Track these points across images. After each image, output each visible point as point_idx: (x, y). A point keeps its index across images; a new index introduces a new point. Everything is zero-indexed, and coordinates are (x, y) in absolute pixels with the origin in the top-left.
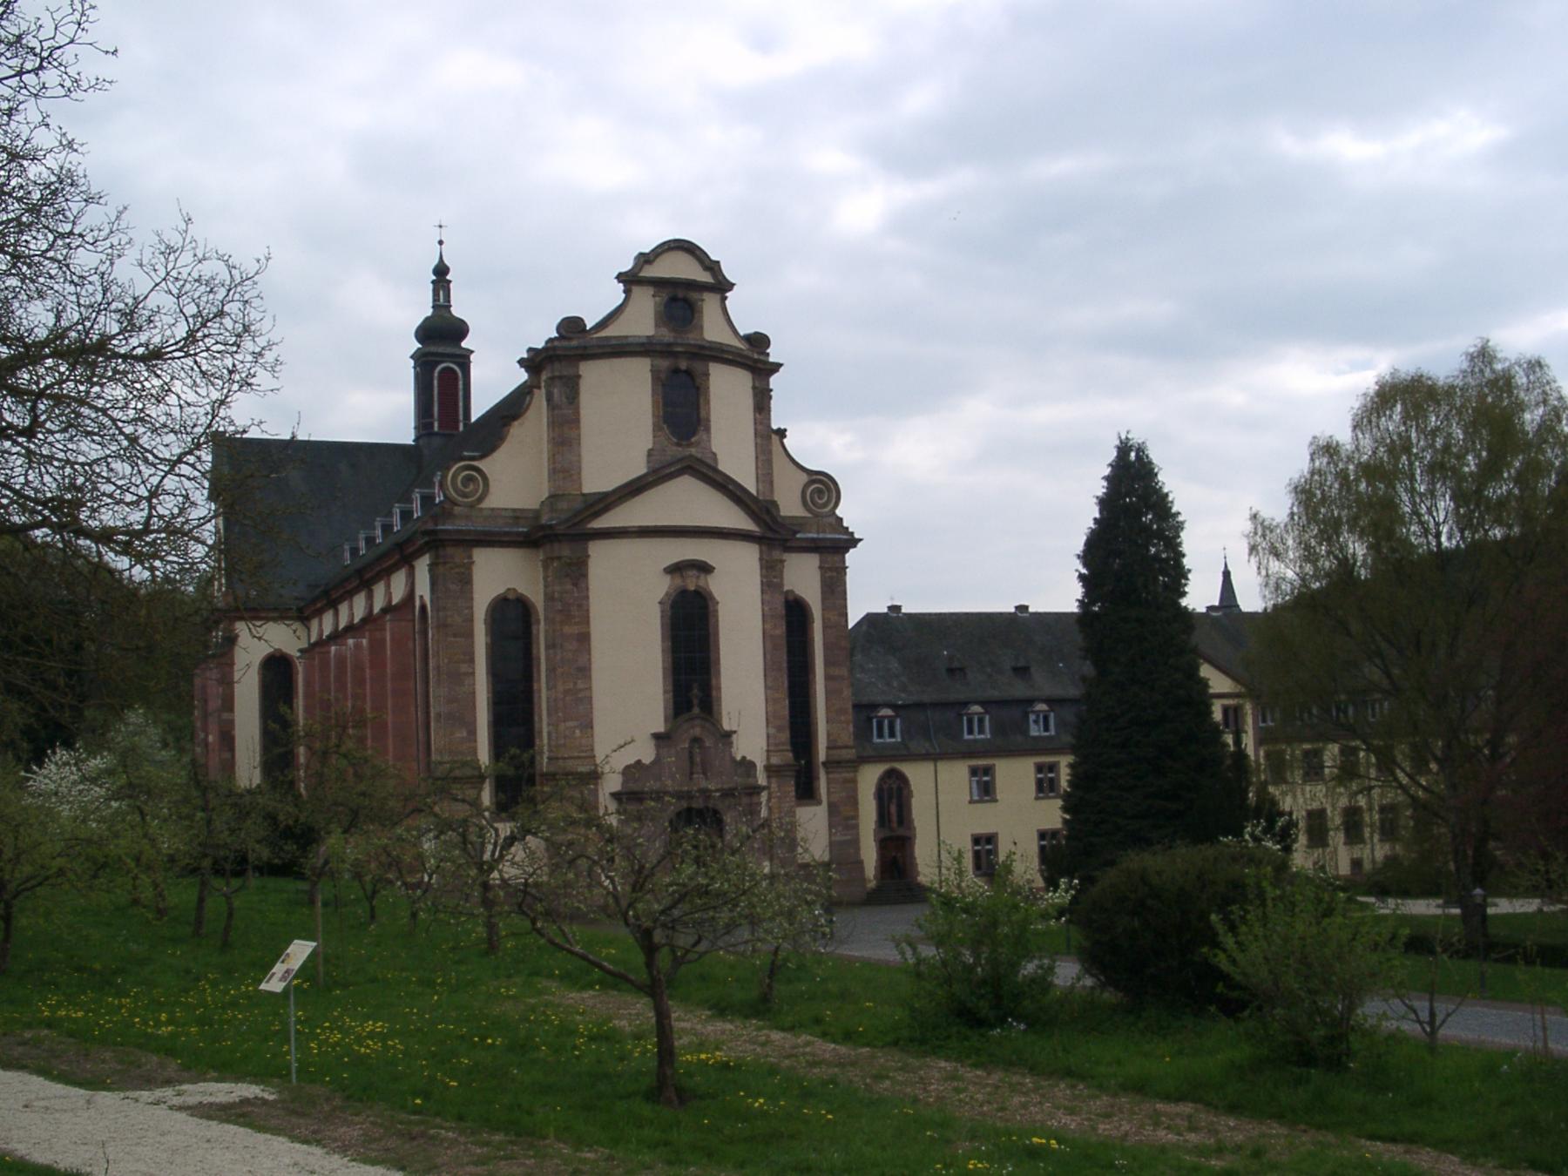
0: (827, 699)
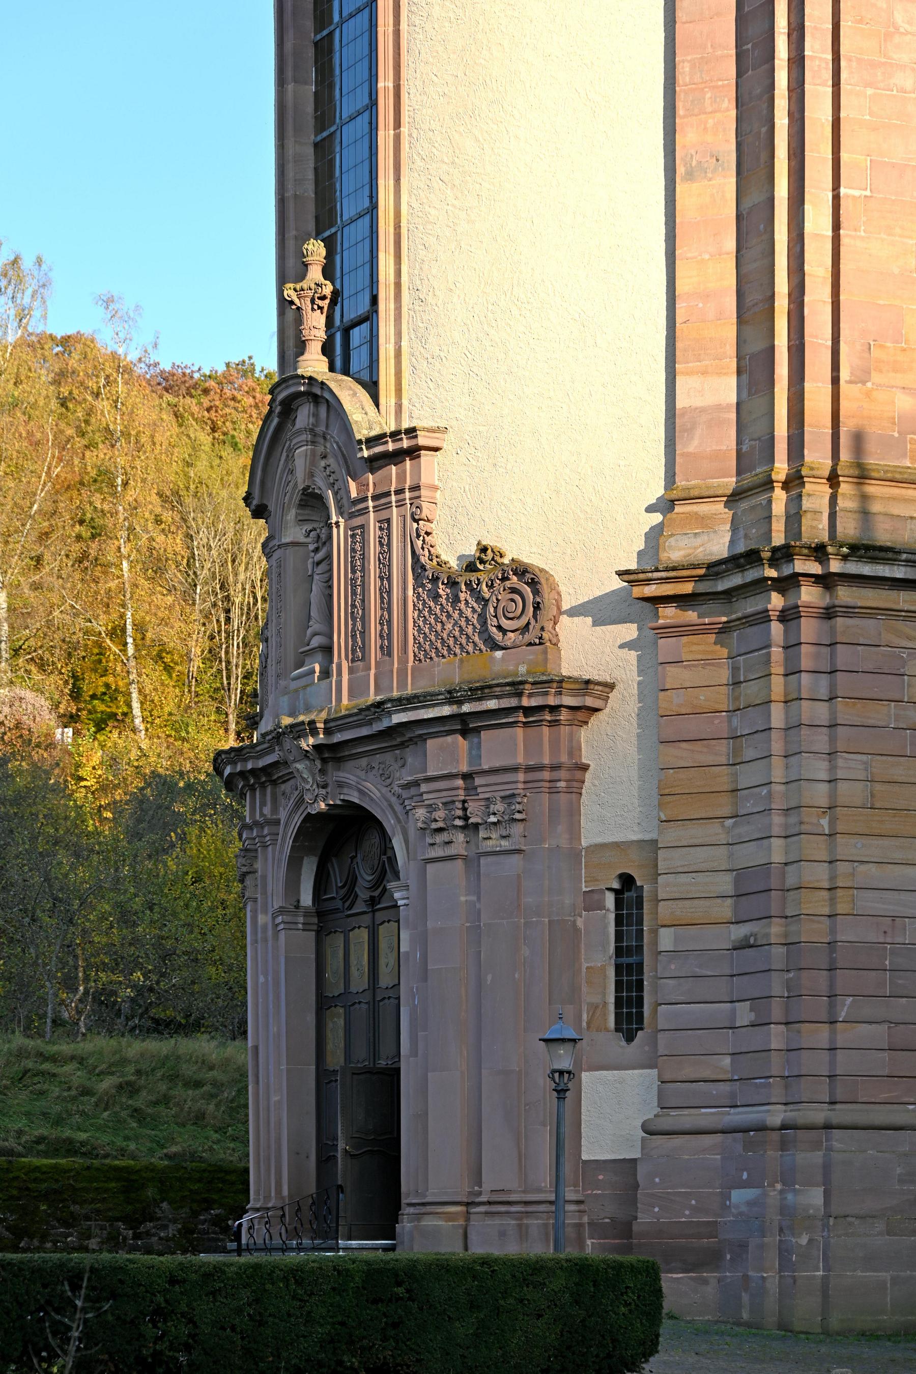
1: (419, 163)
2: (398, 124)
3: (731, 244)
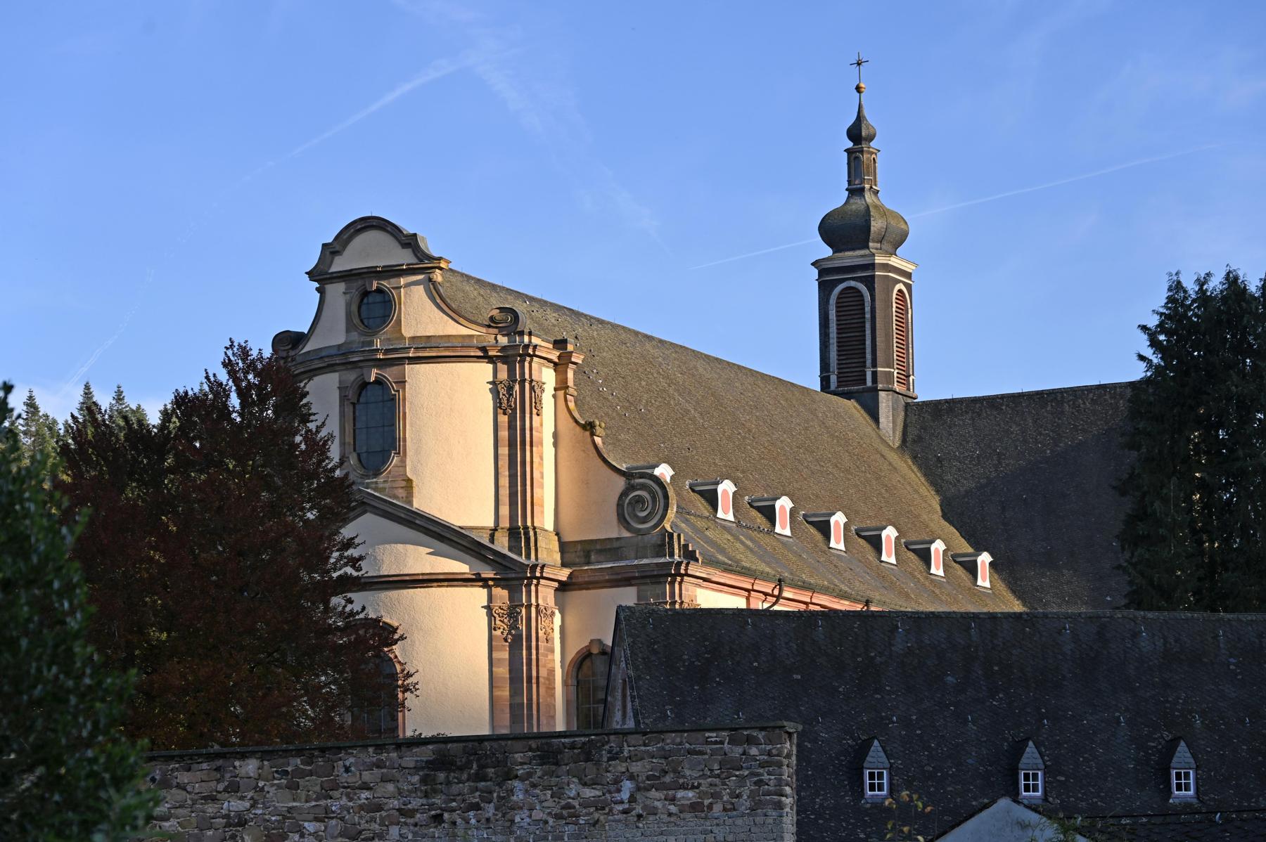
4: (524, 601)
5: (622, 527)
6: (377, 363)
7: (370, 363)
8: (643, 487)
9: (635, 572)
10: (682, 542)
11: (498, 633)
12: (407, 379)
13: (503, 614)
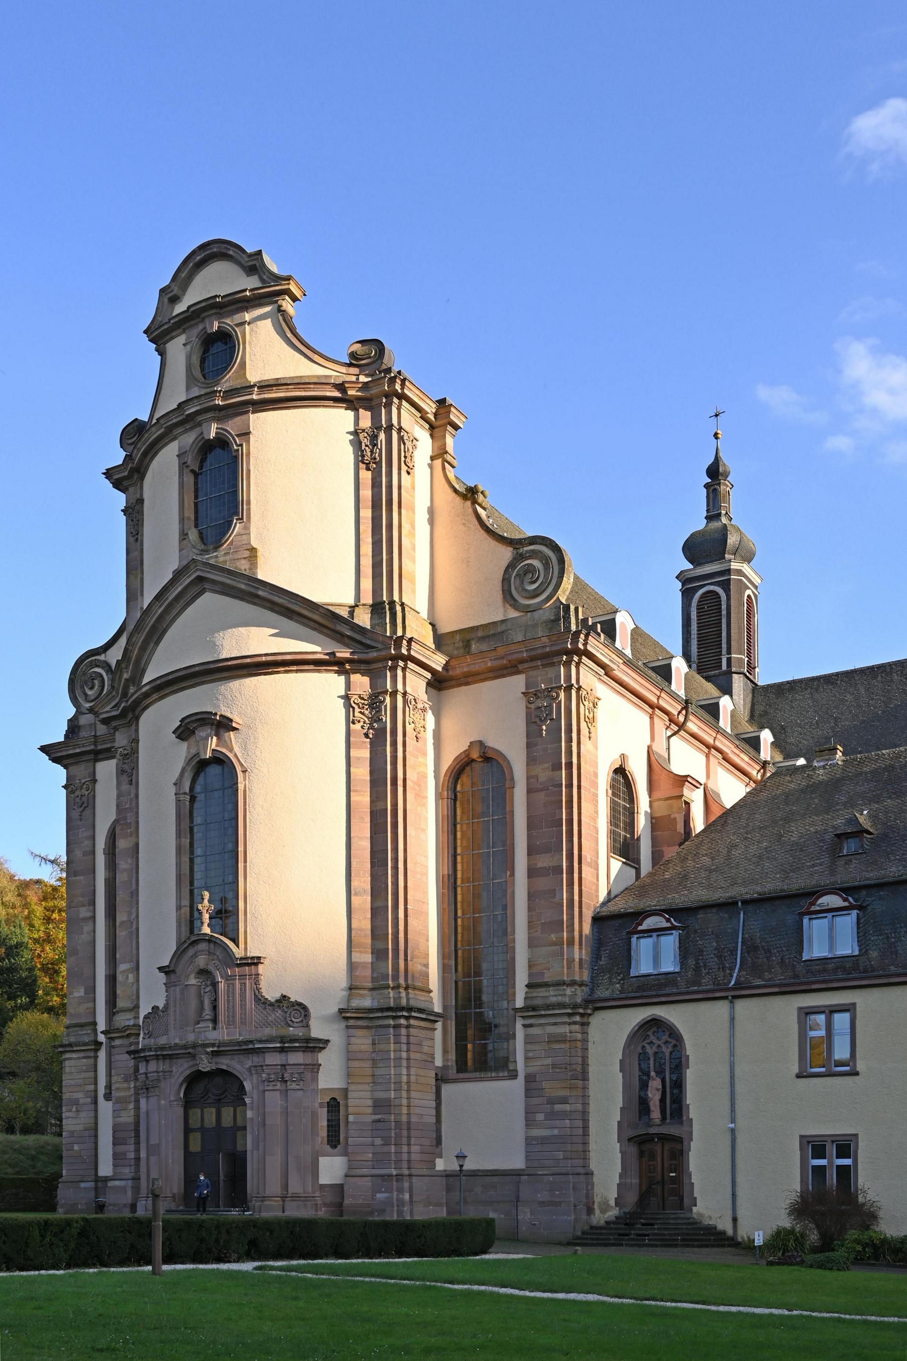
0: (530, 909)
1: (254, 875)
2: (245, 861)
3: (369, 916)
4: (388, 687)
5: (508, 606)
6: (217, 414)
7: (209, 415)
8: (534, 554)
9: (522, 652)
10: (581, 617)
11: (358, 726)
12: (251, 430)
13: (364, 704)
